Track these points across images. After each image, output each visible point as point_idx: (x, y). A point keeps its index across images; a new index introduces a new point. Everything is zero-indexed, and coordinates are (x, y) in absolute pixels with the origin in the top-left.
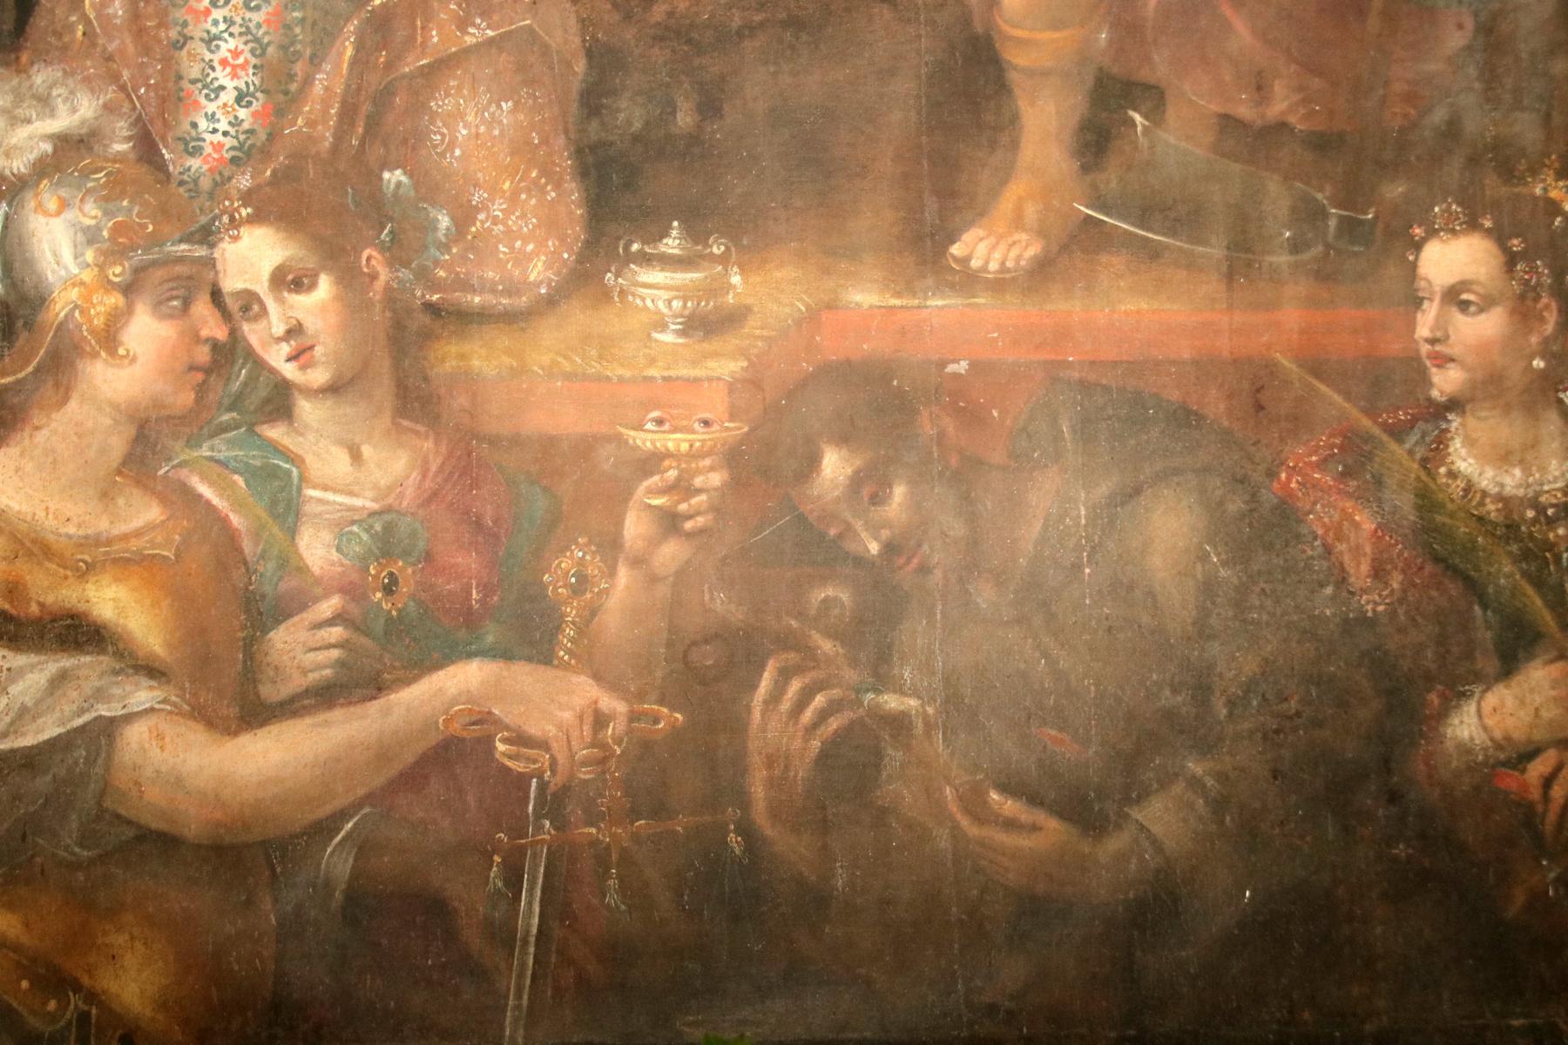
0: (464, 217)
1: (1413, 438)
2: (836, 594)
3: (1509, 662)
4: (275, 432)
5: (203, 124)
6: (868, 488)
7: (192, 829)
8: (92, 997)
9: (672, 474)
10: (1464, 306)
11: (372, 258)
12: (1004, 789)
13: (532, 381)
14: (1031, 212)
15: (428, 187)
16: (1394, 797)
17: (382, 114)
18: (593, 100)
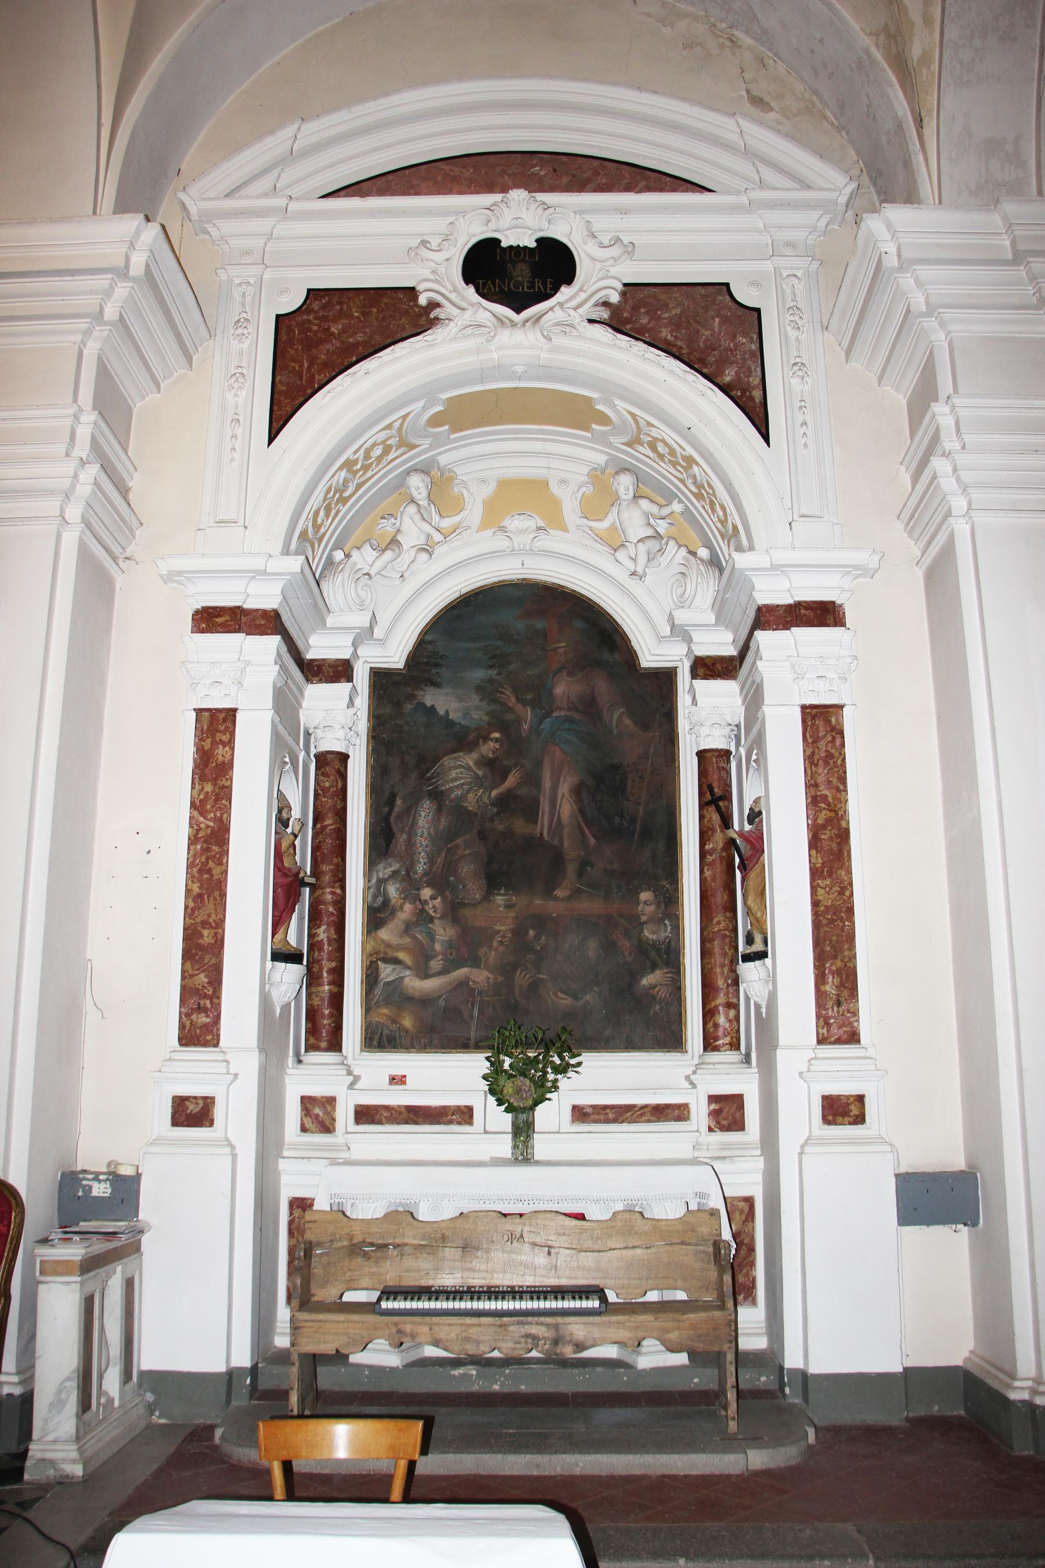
0: (464, 886)
2: (531, 956)
4: (430, 926)
6: (538, 937)
7: (417, 995)
13: (477, 917)
17: (450, 867)
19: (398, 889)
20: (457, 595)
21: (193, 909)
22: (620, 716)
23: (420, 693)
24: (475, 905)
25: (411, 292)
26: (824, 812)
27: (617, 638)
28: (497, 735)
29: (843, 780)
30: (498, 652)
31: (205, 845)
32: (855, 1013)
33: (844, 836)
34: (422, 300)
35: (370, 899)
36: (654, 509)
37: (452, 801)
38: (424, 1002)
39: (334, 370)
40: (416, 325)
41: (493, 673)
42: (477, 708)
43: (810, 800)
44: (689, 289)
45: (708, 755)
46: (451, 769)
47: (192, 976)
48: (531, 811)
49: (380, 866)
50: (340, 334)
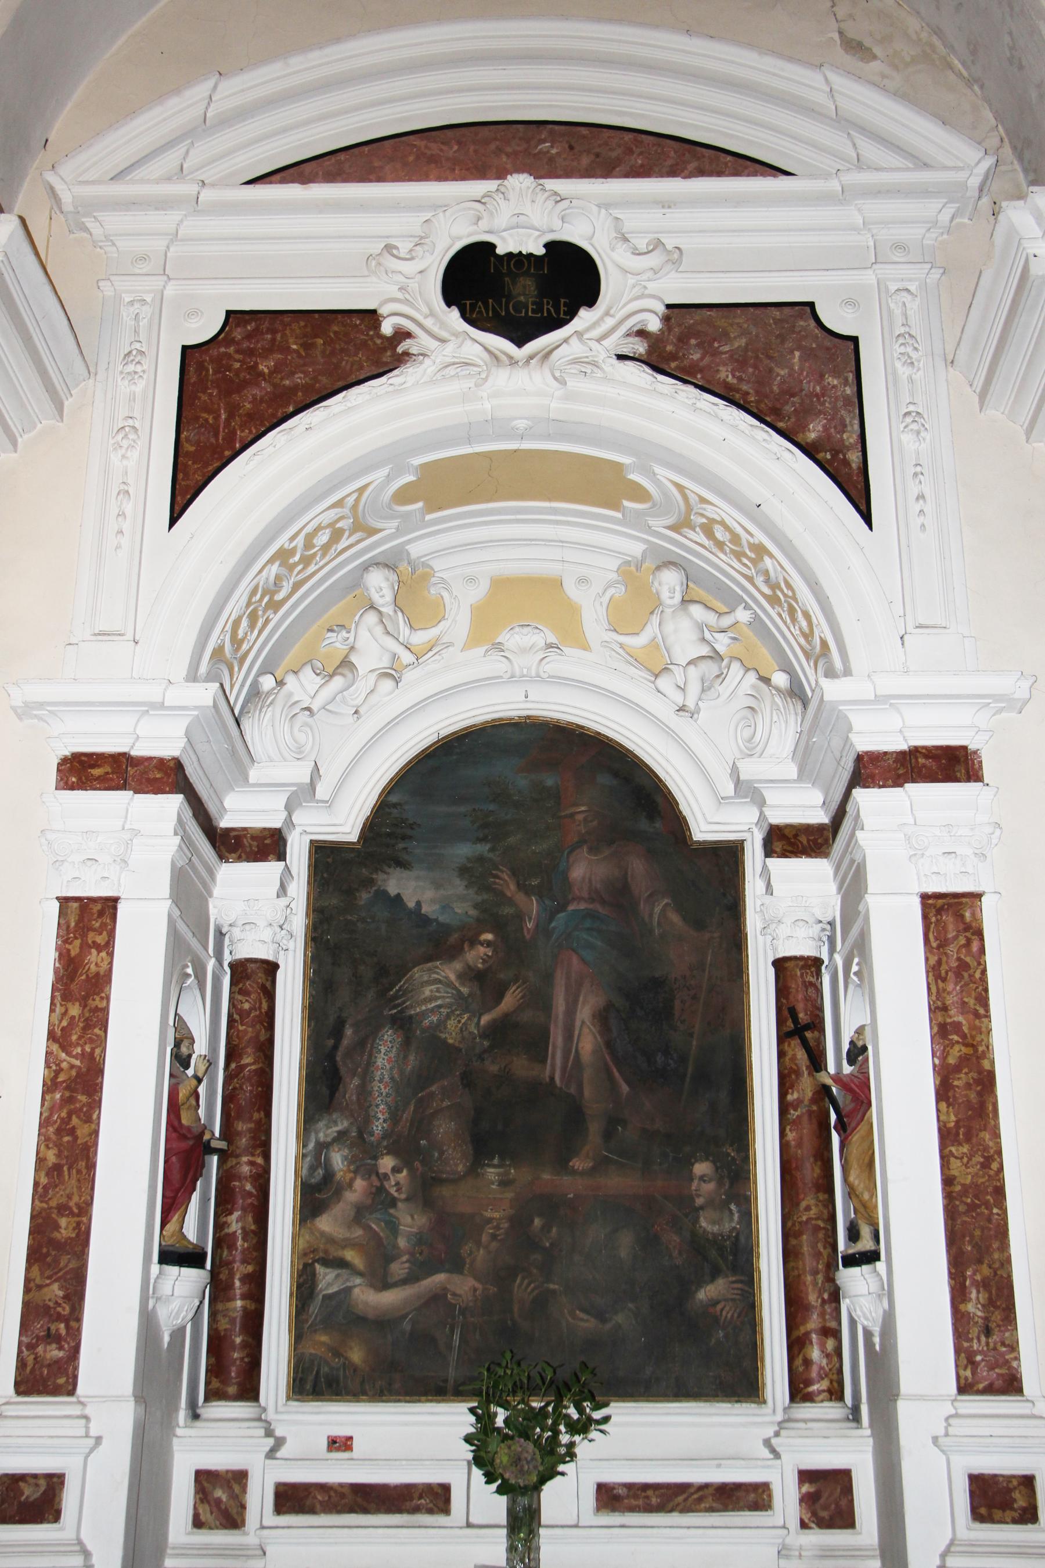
0: (442, 1153)
2: (537, 1257)
3: (713, 1278)
4: (392, 1211)
6: (546, 1228)
7: (371, 1315)
8: (346, 1358)
10: (704, 1181)
11: (417, 1164)
13: (459, 1199)
17: (422, 1125)
19: (345, 1158)
20: (434, 738)
21: (46, 1188)
22: (664, 910)
23: (381, 876)
25: (371, 316)
26: (957, 1048)
27: (659, 800)
28: (489, 936)
29: (983, 1000)
30: (491, 819)
31: (67, 1094)
32: (1014, 1347)
33: (987, 1082)
34: (387, 328)
35: (305, 1172)
36: (711, 618)
38: (381, 1324)
39: (262, 425)
40: (377, 363)
41: (483, 848)
43: (936, 1029)
44: (758, 311)
45: (788, 964)
47: (40, 1287)
48: (537, 1045)
49: (321, 1124)
50: (271, 373)
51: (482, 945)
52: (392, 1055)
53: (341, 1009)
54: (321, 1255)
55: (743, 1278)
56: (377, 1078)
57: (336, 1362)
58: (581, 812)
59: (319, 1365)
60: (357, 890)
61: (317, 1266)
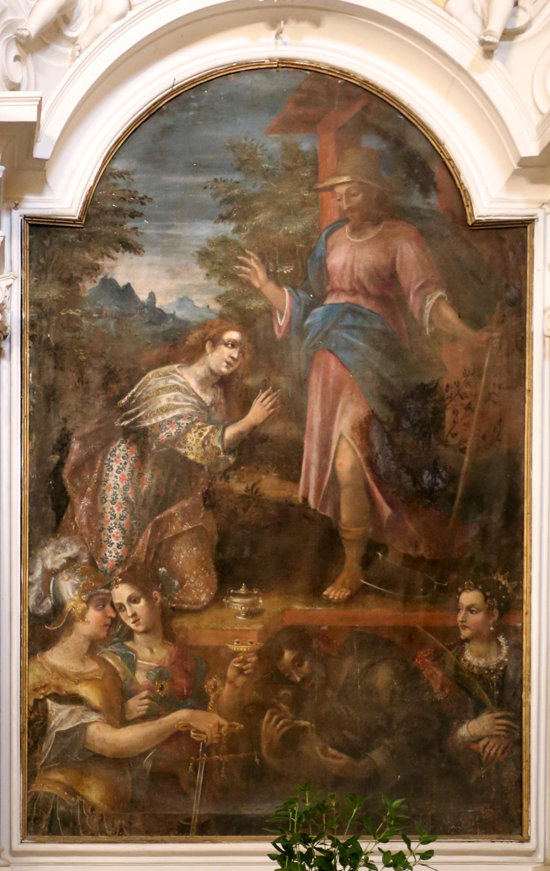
0: (182, 582)
1: (454, 651)
3: (477, 714)
4: (129, 644)
5: (108, 554)
6: (297, 662)
8: (83, 797)
9: (241, 657)
10: (472, 612)
11: (156, 594)
12: (332, 747)
13: (201, 630)
14: (348, 582)
15: (172, 572)
16: (442, 751)
17: (160, 551)
18: (220, 547)
19: (77, 587)
22: (436, 306)
23: (105, 263)
24: (197, 611)
27: (436, 168)
30: (236, 192)
35: (32, 602)
37: (161, 445)
38: (120, 761)
41: (227, 229)
42: (202, 289)
46: (159, 391)
48: (289, 462)
49: (48, 550)
51: (226, 345)
52: (126, 472)
53: (65, 420)
54: (53, 690)
55: (509, 714)
56: (109, 499)
57: (72, 801)
58: (343, 185)
59: (55, 804)
60: (80, 279)
61: (49, 702)
